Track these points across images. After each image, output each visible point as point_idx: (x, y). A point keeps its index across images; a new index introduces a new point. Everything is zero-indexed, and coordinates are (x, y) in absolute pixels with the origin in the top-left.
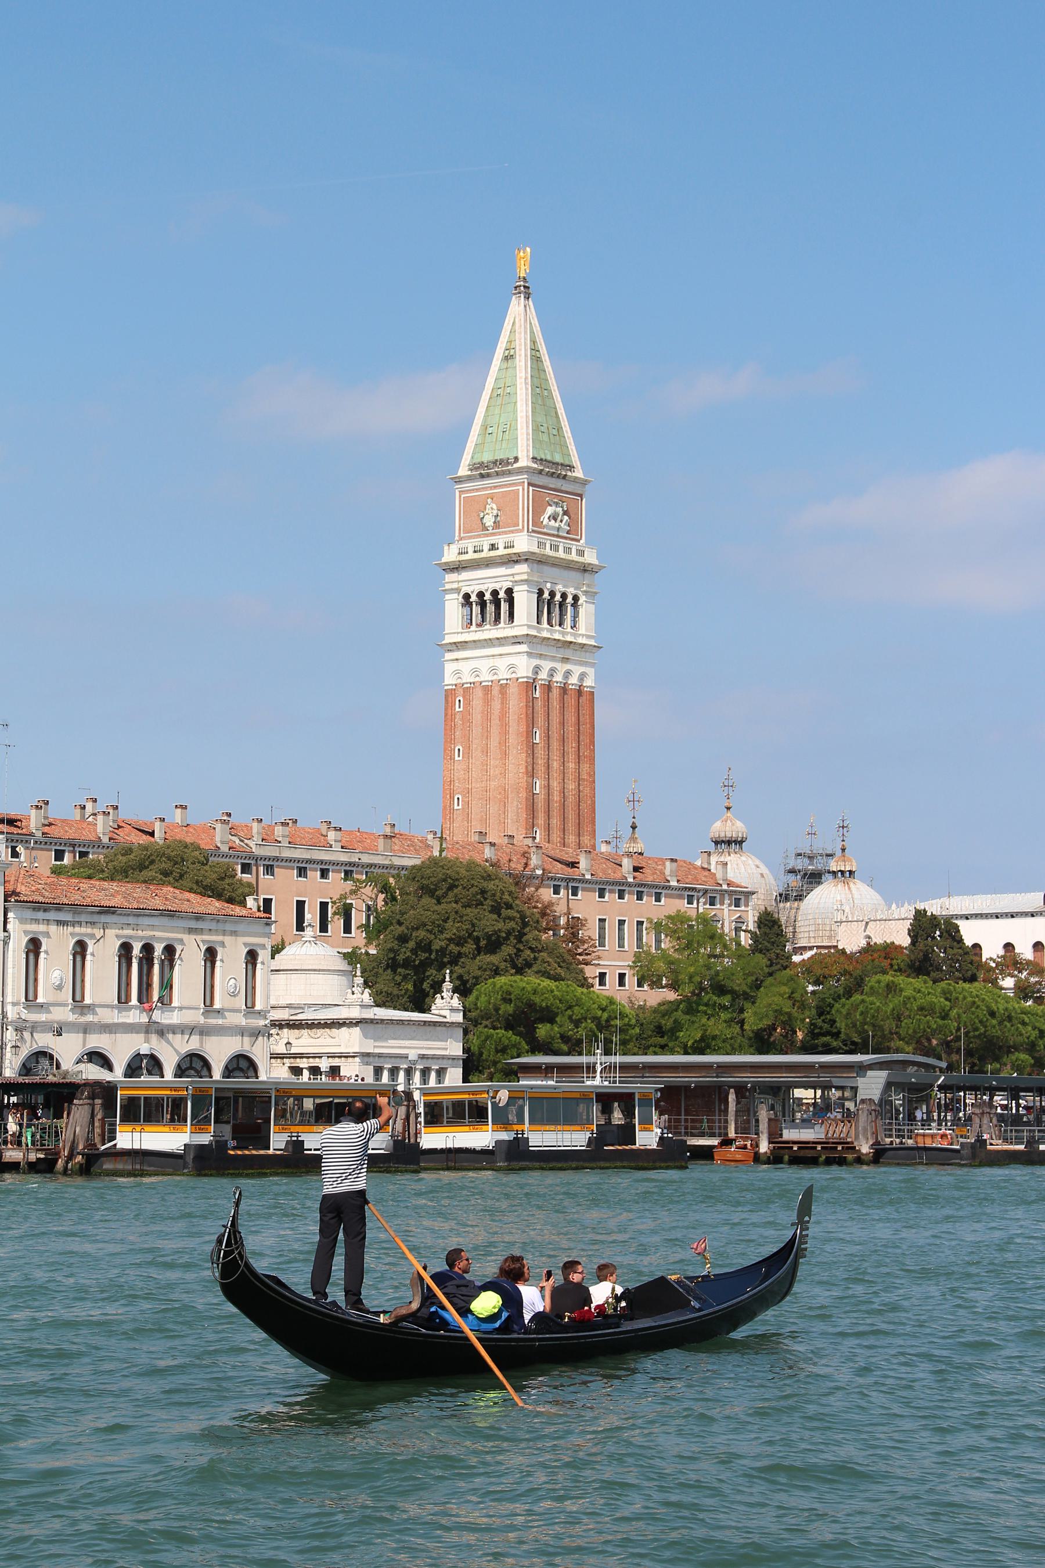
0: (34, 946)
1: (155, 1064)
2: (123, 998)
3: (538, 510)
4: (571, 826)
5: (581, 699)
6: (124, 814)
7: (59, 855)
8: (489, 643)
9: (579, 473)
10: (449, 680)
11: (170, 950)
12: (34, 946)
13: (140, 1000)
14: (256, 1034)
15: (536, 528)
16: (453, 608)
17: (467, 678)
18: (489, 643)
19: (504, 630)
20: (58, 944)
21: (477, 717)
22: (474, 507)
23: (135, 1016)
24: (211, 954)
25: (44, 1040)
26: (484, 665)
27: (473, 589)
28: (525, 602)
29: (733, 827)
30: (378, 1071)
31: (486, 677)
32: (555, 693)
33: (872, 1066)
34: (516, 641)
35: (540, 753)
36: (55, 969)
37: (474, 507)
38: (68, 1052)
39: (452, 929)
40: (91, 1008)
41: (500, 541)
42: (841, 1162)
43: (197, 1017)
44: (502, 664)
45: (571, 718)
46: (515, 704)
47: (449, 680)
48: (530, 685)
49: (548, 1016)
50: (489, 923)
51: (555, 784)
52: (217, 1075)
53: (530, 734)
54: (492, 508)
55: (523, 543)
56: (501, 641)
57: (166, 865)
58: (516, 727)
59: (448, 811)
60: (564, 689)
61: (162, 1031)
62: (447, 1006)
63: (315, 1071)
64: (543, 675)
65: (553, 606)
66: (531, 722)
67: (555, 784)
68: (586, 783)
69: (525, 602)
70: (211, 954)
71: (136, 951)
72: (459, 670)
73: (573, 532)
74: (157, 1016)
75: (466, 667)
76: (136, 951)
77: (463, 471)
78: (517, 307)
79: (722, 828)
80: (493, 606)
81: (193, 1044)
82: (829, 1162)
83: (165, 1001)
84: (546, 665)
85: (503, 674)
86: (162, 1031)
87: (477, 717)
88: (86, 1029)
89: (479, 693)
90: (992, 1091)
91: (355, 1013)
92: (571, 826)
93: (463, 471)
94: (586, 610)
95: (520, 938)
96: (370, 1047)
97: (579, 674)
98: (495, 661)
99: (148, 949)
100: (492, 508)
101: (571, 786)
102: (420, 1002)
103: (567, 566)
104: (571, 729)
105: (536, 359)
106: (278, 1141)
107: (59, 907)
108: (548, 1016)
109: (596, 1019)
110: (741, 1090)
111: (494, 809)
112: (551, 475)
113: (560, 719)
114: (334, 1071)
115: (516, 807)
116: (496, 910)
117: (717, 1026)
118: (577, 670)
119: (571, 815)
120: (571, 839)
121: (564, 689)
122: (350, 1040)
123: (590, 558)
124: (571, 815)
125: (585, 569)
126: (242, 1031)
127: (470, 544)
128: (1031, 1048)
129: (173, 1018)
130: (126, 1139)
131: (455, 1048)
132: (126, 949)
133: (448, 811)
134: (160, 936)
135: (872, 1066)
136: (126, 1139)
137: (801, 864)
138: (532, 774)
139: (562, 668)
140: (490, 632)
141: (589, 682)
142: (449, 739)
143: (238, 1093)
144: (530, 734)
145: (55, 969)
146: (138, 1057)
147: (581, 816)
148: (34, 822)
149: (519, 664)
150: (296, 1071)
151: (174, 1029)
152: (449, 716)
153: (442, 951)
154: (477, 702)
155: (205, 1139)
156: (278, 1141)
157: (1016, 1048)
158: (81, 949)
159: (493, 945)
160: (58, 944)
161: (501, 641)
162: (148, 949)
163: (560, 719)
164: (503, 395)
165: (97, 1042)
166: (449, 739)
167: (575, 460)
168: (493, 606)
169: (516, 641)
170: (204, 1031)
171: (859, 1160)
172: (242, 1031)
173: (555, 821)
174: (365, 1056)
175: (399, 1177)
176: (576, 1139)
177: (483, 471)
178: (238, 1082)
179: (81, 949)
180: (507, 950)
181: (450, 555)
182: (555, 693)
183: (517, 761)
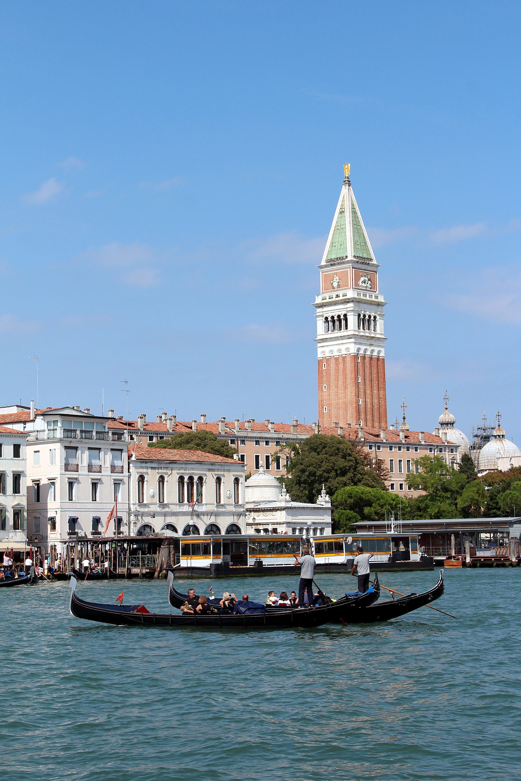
0: (141, 479)
1: (196, 529)
2: (181, 501)
3: (357, 279)
4: (376, 419)
6: (178, 420)
7: (151, 438)
8: (337, 338)
9: (374, 262)
10: (320, 355)
11: (201, 479)
12: (141, 479)
13: (188, 501)
14: (239, 515)
15: (356, 287)
16: (321, 324)
17: (328, 354)
18: (337, 338)
19: (343, 333)
20: (152, 477)
21: (333, 372)
22: (329, 279)
23: (186, 508)
24: (219, 480)
25: (147, 520)
27: (329, 315)
28: (352, 320)
29: (449, 417)
30: (294, 530)
31: (336, 354)
32: (367, 360)
34: (349, 337)
35: (361, 386)
36: (151, 488)
37: (329, 279)
38: (158, 525)
39: (325, 466)
40: (167, 505)
41: (341, 293)
42: (503, 566)
43: (213, 508)
44: (343, 347)
45: (374, 371)
46: (350, 365)
48: (356, 357)
49: (369, 504)
50: (341, 463)
51: (368, 400)
52: (223, 533)
53: (356, 378)
54: (336, 279)
55: (351, 294)
56: (342, 338)
58: (350, 375)
60: (371, 358)
62: (324, 500)
63: (266, 530)
64: (362, 352)
65: (365, 321)
68: (382, 399)
69: (352, 320)
70: (219, 480)
71: (186, 480)
72: (324, 351)
74: (196, 508)
76: (186, 480)
77: (323, 263)
78: (345, 190)
79: (443, 418)
80: (338, 322)
81: (212, 520)
82: (498, 566)
83: (199, 501)
84: (363, 348)
85: (344, 352)
87: (333, 372)
88: (165, 515)
89: (333, 361)
91: (283, 504)
92: (376, 419)
93: (323, 263)
94: (380, 323)
96: (290, 519)
97: (377, 351)
98: (341, 347)
99: (191, 478)
100: (336, 279)
101: (376, 401)
102: (312, 499)
103: (371, 303)
104: (375, 375)
105: (354, 212)
106: (251, 562)
107: (152, 461)
108: (369, 504)
109: (390, 504)
110: (457, 535)
111: (341, 412)
112: (362, 264)
113: (370, 371)
114: (275, 531)
116: (344, 457)
117: (445, 506)
118: (377, 349)
119: (376, 414)
120: (376, 424)
121: (371, 358)
122: (281, 516)
123: (381, 299)
124: (376, 414)
125: (379, 304)
126: (233, 514)
127: (327, 296)
130: (185, 562)
132: (181, 478)
133: (321, 414)
136: (185, 562)
137: (480, 433)
138: (358, 396)
139: (370, 349)
140: (337, 334)
141: (382, 354)
142: (320, 383)
143: (233, 541)
144: (356, 378)
145: (151, 488)
146: (188, 526)
147: (380, 414)
148: (139, 424)
150: (258, 531)
151: (204, 514)
152: (320, 372)
153: (321, 476)
155: (219, 561)
156: (251, 562)
158: (162, 479)
159: (343, 472)
160: (152, 477)
161: (342, 338)
162: (191, 478)
163: (370, 371)
164: (340, 229)
165: (170, 520)
166: (320, 383)
167: (373, 256)
168: (338, 322)
169: (349, 337)
170: (217, 514)
171: (512, 565)
172: (233, 514)
173: (369, 417)
174: (288, 523)
177: (332, 263)
178: (232, 536)
179: (162, 479)
180: (350, 475)
181: (319, 300)
182: (367, 360)
183: (351, 391)
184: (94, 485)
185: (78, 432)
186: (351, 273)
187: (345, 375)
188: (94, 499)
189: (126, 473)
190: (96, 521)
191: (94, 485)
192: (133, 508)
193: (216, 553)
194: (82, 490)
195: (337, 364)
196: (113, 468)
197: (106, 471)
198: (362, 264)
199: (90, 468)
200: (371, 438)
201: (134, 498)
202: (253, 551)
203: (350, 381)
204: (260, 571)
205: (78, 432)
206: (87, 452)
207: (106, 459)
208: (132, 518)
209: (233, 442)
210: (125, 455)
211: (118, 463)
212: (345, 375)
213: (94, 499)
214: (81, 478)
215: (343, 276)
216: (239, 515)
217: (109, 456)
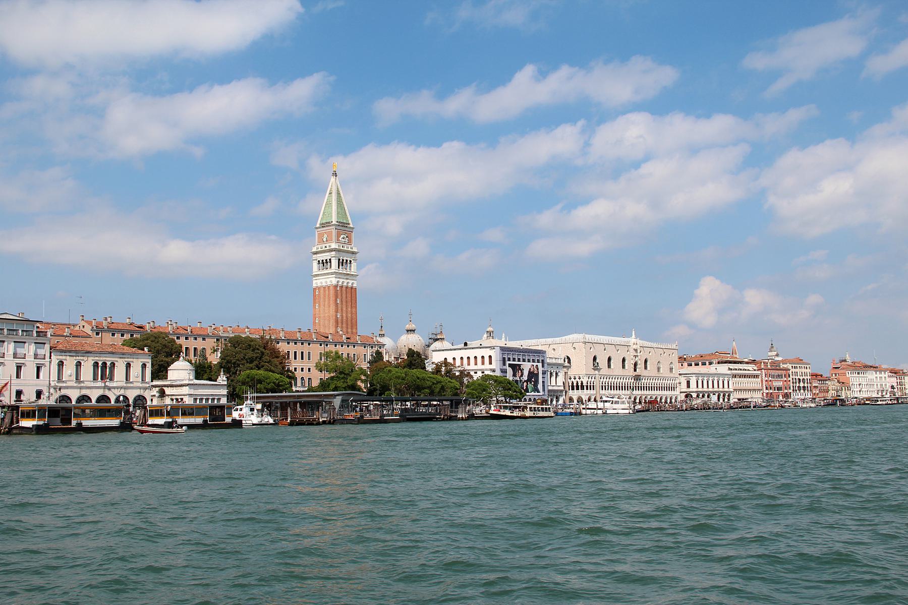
0: (61, 364)
1: (89, 399)
2: (95, 378)
3: (338, 236)
4: (349, 327)
5: (352, 291)
6: (179, 325)
7: (123, 335)
8: (325, 274)
9: (351, 226)
10: (314, 285)
11: (113, 365)
12: (61, 364)
13: (102, 379)
14: (145, 389)
15: (338, 241)
16: (315, 264)
17: (319, 285)
18: (325, 274)
21: (322, 296)
23: (100, 384)
24: (128, 366)
25: (64, 392)
26: (323, 281)
27: (320, 259)
29: (412, 326)
30: (195, 400)
31: (324, 284)
32: (344, 289)
33: (338, 395)
34: (332, 274)
35: (339, 306)
36: (69, 370)
38: (74, 395)
40: (83, 382)
41: (327, 245)
44: (328, 280)
45: (349, 296)
46: (332, 292)
47: (314, 285)
48: (336, 286)
50: (250, 354)
51: (344, 315)
52: (74, 403)
53: (336, 300)
54: (325, 236)
55: (334, 246)
56: (328, 274)
57: (153, 339)
58: (332, 298)
59: (314, 323)
60: (347, 287)
61: (109, 389)
63: (177, 399)
64: (340, 283)
65: (341, 263)
66: (336, 297)
67: (344, 315)
69: (334, 263)
70: (128, 366)
71: (100, 364)
72: (317, 282)
73: (350, 242)
74: (107, 384)
75: (318, 281)
76: (100, 364)
77: (318, 226)
78: (333, 179)
79: (408, 327)
80: (325, 263)
81: (122, 392)
82: (308, 424)
83: (111, 379)
84: (341, 280)
85: (329, 283)
86: (109, 389)
87: (322, 296)
88: (81, 388)
90: (406, 401)
91: (187, 382)
92: (349, 327)
93: (318, 226)
94: (354, 264)
95: (260, 359)
96: (192, 392)
99: (104, 364)
100: (325, 236)
101: (349, 315)
103: (348, 252)
104: (349, 299)
105: (338, 194)
106: (74, 423)
107: (76, 352)
108: (260, 381)
109: (274, 383)
110: (300, 402)
111: (327, 322)
112: (343, 227)
113: (346, 296)
114: (182, 399)
115: (332, 322)
116: (253, 350)
118: (351, 282)
119: (349, 323)
120: (349, 330)
121: (347, 287)
122: (186, 390)
123: (355, 250)
124: (349, 323)
125: (353, 253)
126: (140, 388)
127: (319, 246)
128: (430, 388)
129: (115, 384)
130: (151, 421)
131: (224, 392)
132: (96, 365)
133: (314, 323)
134: (109, 360)
135: (338, 395)
136: (151, 421)
137: (434, 336)
138: (337, 312)
139: (346, 281)
140: (325, 271)
141: (355, 285)
142: (315, 303)
143: (63, 408)
144: (336, 300)
145: (69, 370)
146: (139, 396)
147: (352, 323)
149: (333, 280)
150: (172, 400)
151: (114, 388)
152: (314, 296)
153: (234, 363)
154: (322, 291)
155: (41, 423)
156: (74, 423)
157: (425, 388)
158: (79, 365)
161: (328, 274)
162: (104, 364)
163: (346, 296)
164: (329, 204)
165: (85, 392)
167: (350, 222)
169: (332, 274)
170: (125, 388)
172: (140, 388)
173: (344, 325)
174: (190, 395)
175: (125, 434)
176: (199, 420)
177: (323, 225)
178: (64, 405)
179: (79, 365)
180: (255, 363)
181: (314, 250)
182: (344, 289)
183: (333, 307)
184: (38, 369)
185: (5, 331)
186: (334, 232)
187: (329, 298)
188: (38, 377)
189: (47, 359)
190: (19, 393)
191: (38, 369)
192: (52, 384)
193: (41, 417)
194: (29, 371)
195: (325, 291)
196: (36, 356)
197: (30, 358)
198: (343, 227)
199: (15, 356)
200: (323, 339)
201: (54, 376)
202: (76, 416)
203: (332, 302)
204: (80, 428)
205: (5, 331)
206: (13, 344)
207: (30, 349)
208: (52, 390)
209: (178, 338)
210: (47, 346)
211: (41, 352)
212: (329, 298)
213: (38, 377)
214: (27, 363)
215: (329, 234)
216: (145, 389)
217: (33, 347)
